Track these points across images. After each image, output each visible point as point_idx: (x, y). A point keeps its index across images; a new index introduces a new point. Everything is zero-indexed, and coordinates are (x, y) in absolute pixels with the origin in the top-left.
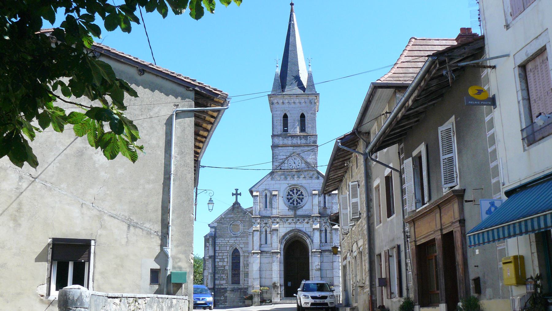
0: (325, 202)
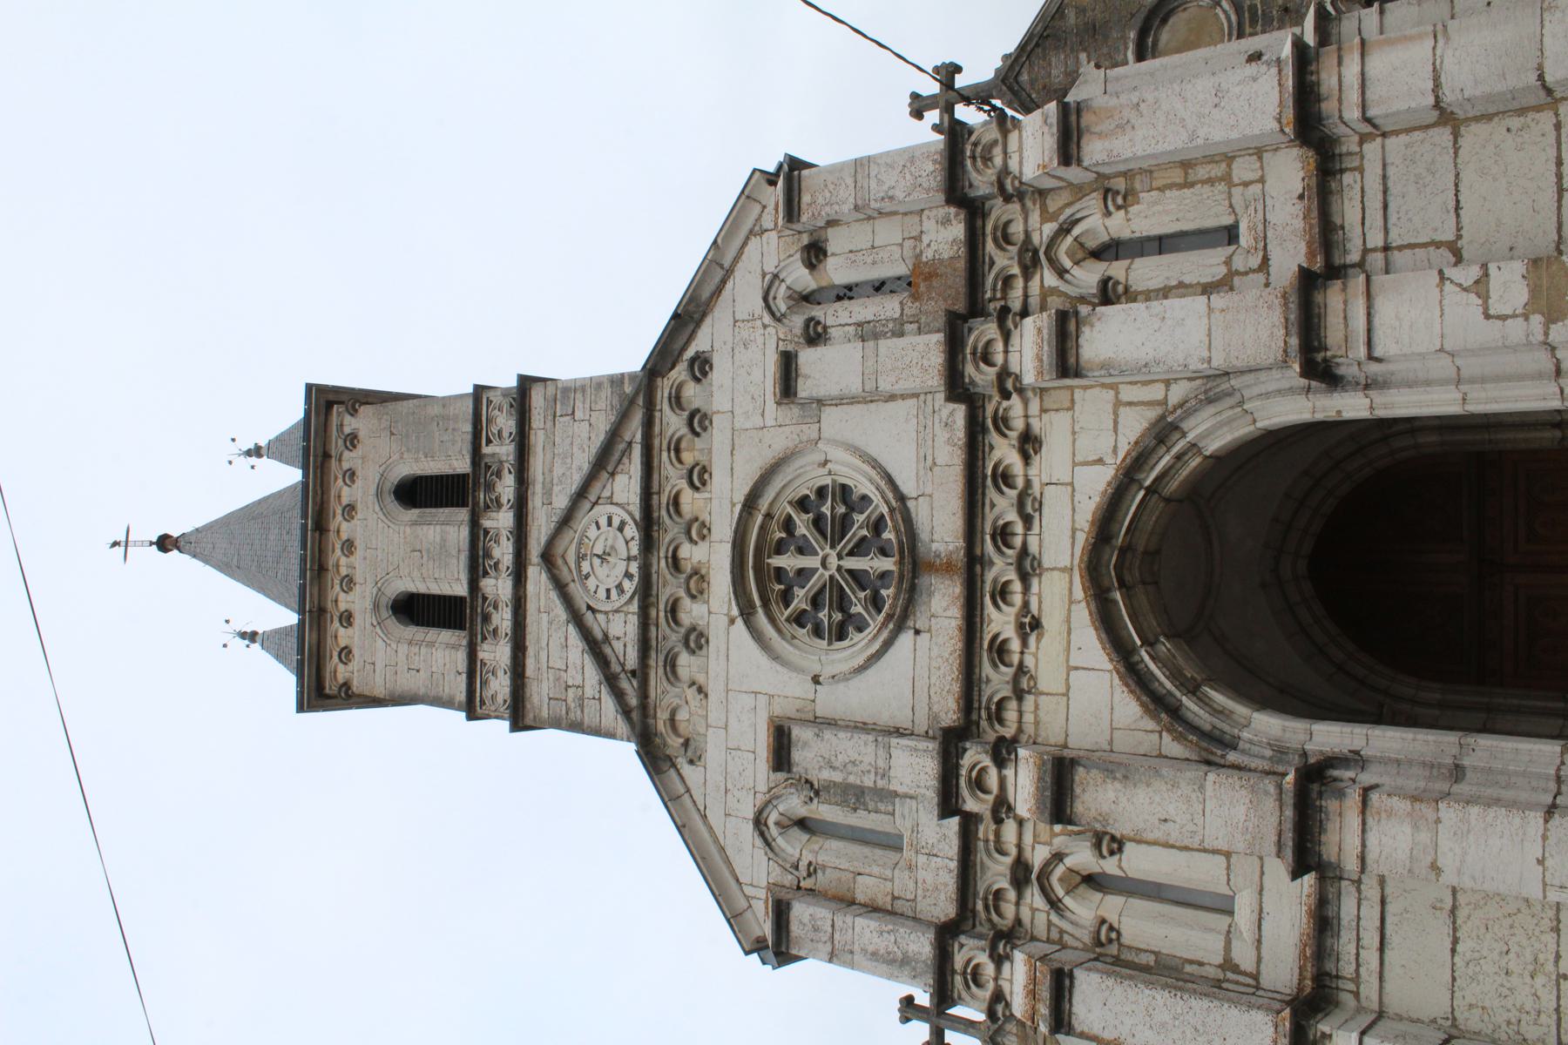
0: (879, 287)
